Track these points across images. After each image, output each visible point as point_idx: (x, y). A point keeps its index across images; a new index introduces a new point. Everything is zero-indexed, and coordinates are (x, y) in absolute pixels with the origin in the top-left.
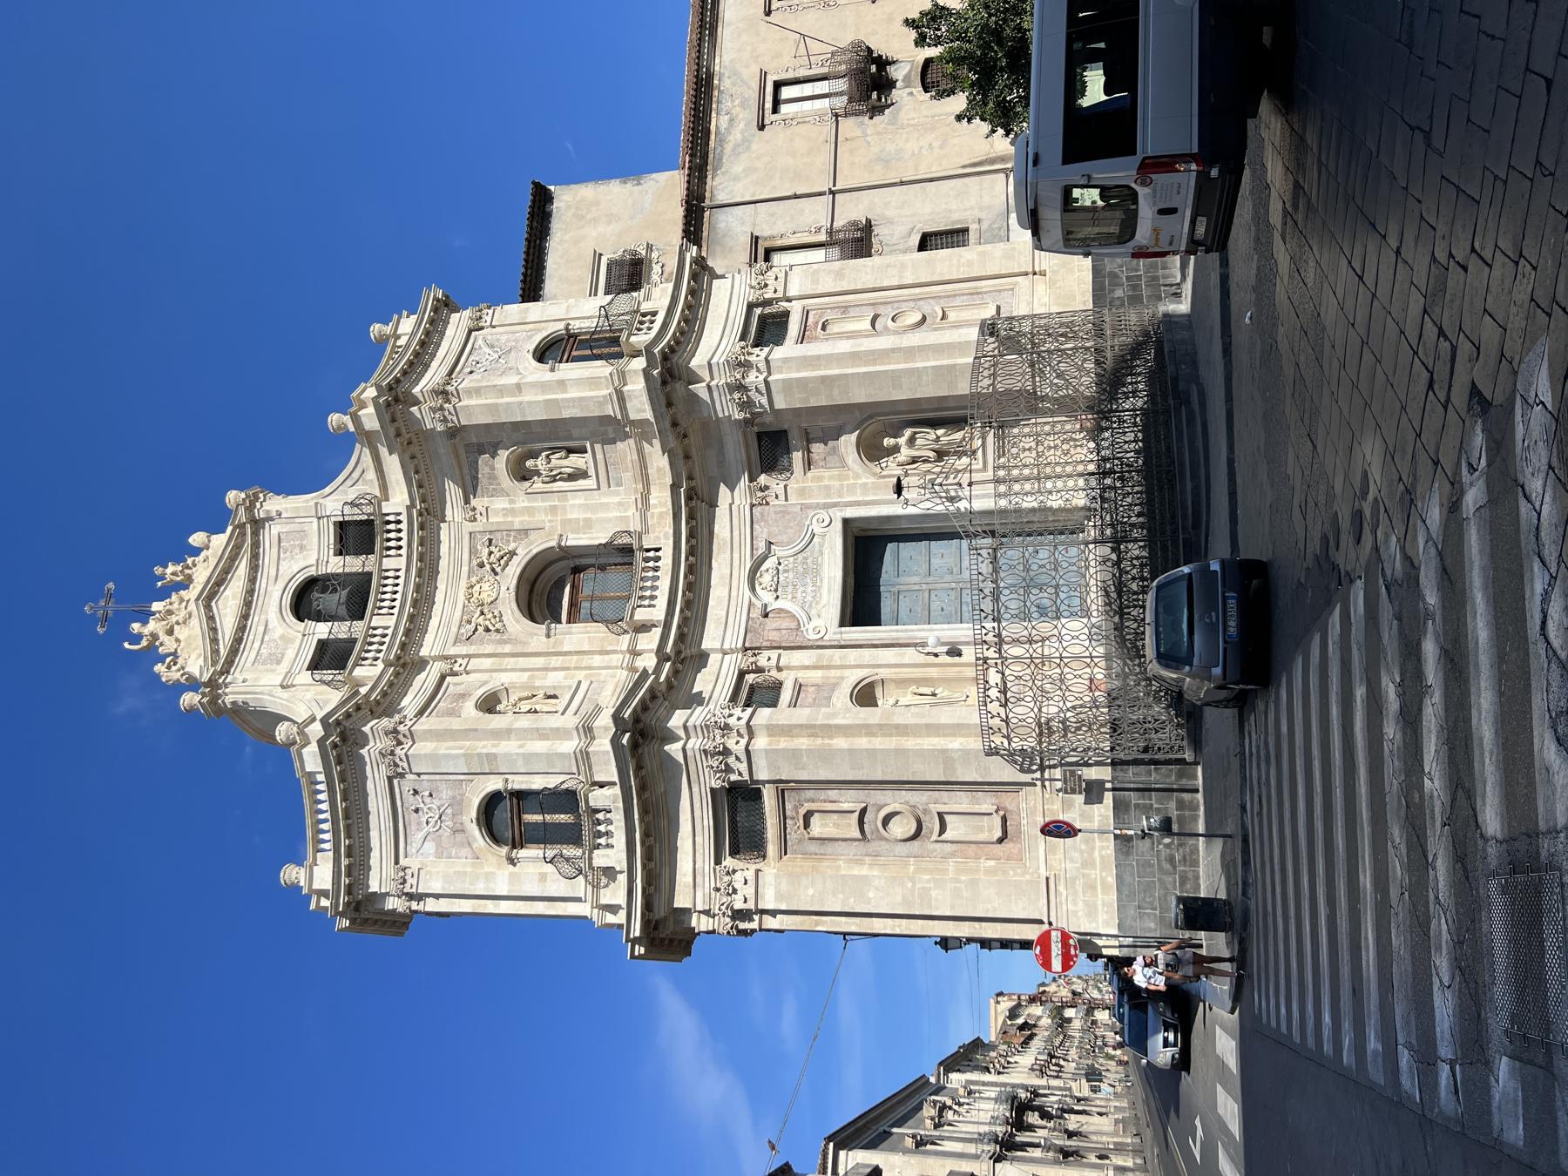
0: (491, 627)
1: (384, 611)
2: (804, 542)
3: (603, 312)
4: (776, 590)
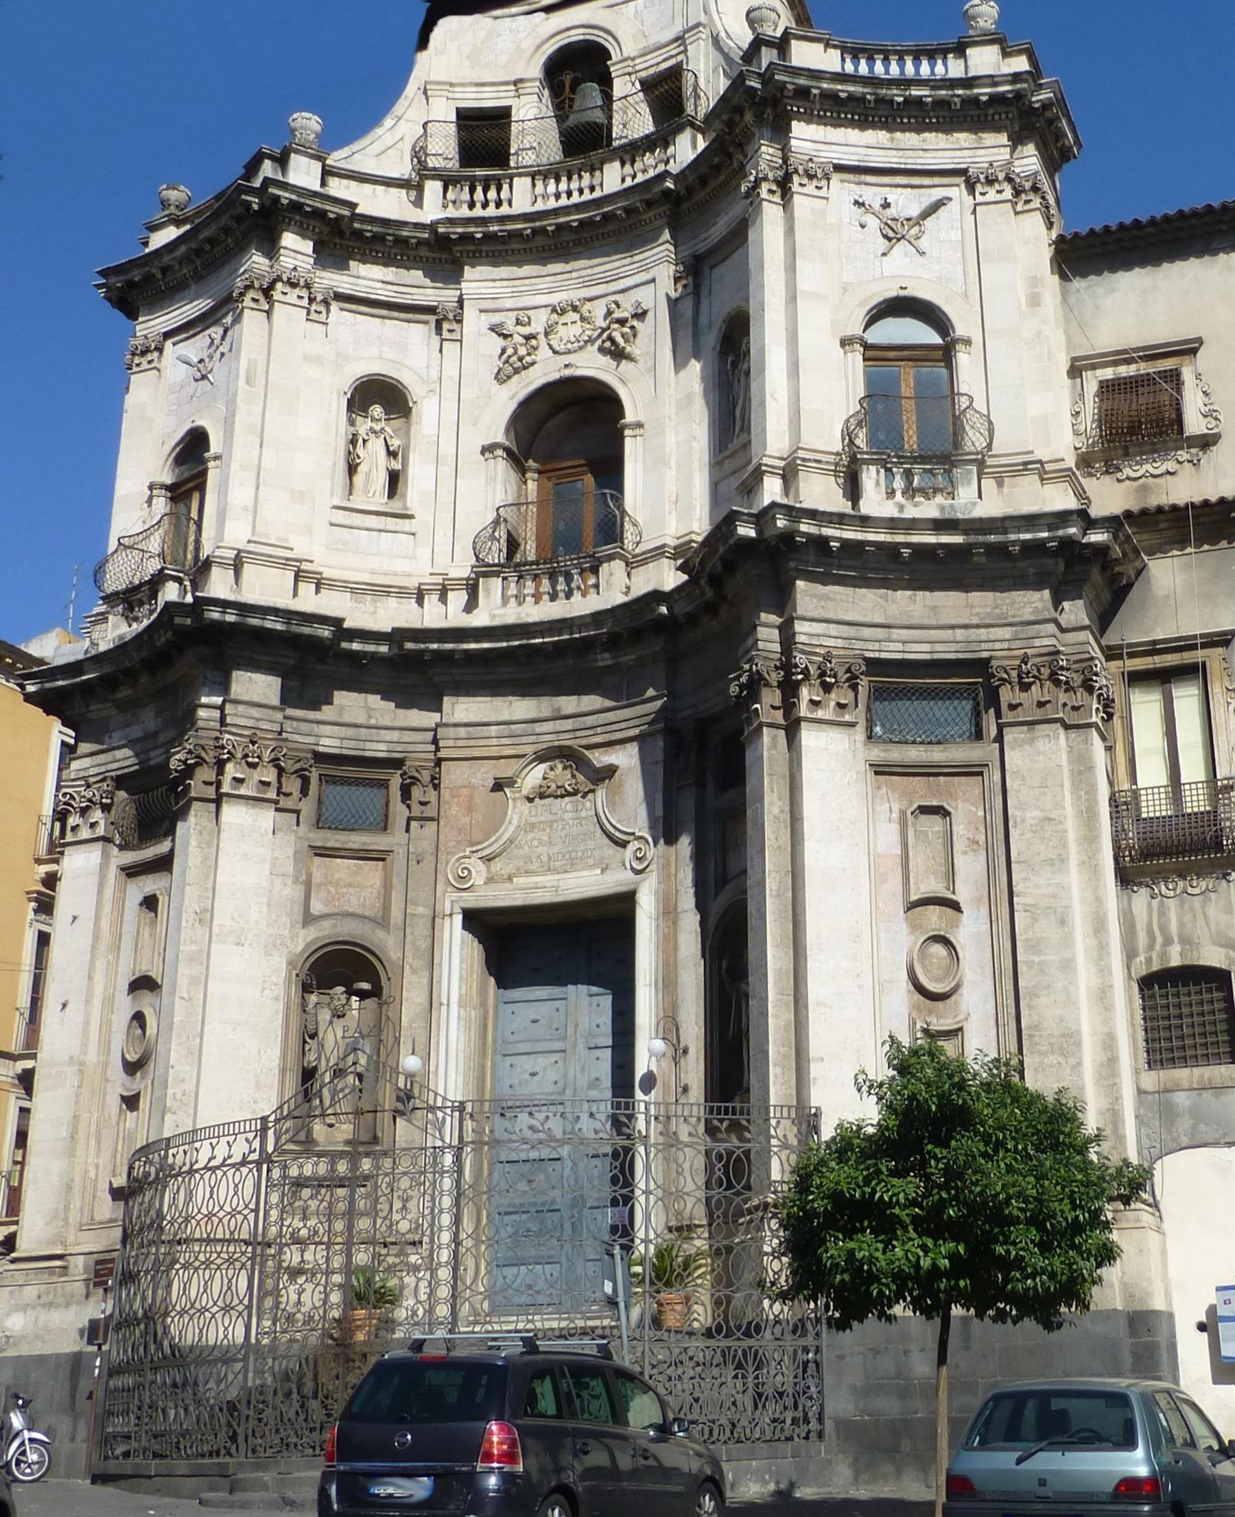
2: (612, 830)
4: (542, 796)
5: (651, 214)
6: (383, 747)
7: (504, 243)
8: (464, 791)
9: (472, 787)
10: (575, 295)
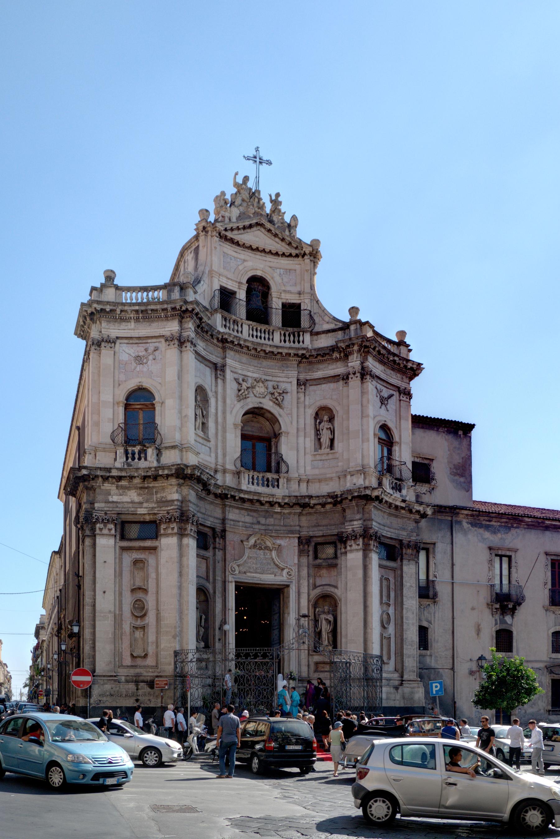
0: (240, 393)
1: (251, 332)
3: (403, 463)
5: (294, 358)
6: (209, 523)
7: (242, 348)
8: (232, 542)
9: (234, 541)
10: (264, 377)
